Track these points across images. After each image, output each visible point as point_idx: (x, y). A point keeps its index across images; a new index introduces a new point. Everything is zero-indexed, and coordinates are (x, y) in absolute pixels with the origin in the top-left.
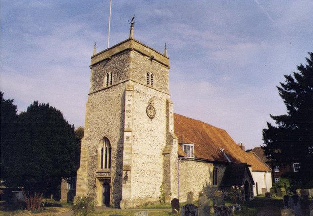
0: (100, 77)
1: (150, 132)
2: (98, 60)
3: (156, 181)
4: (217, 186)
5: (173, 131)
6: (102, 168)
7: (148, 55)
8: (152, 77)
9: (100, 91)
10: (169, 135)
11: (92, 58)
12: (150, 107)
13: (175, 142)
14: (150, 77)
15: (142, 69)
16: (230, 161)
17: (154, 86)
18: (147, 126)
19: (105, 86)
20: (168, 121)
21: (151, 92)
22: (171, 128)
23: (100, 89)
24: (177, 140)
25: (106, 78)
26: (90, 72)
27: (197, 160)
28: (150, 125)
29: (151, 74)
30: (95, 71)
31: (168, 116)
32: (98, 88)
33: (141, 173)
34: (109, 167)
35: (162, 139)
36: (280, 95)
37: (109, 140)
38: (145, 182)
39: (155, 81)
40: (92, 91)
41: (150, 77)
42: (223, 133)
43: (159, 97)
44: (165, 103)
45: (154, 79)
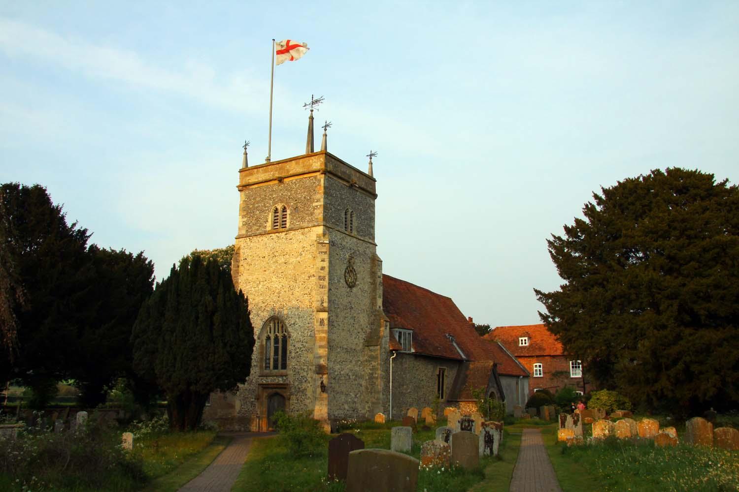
0: (262, 211)
1: (349, 310)
2: (253, 179)
3: (357, 391)
4: (442, 400)
5: (382, 308)
6: (267, 367)
7: (346, 178)
8: (351, 217)
9: (261, 234)
10: (373, 312)
11: (241, 171)
12: (350, 270)
13: (386, 326)
14: (349, 216)
15: (339, 205)
16: (464, 357)
17: (354, 233)
18: (345, 301)
19: (269, 226)
20: (374, 290)
21: (349, 242)
22: (380, 302)
23: (258, 232)
24: (388, 324)
25: (270, 218)
26: (236, 199)
27: (416, 356)
28: (350, 299)
29: (350, 211)
30: (248, 197)
31: (373, 283)
32: (258, 230)
33: (337, 378)
34: (284, 366)
35: (364, 319)
36: (553, 257)
37: (283, 322)
38: (342, 392)
39: (355, 224)
40: (244, 232)
41: (349, 216)
42: (446, 304)
43: (361, 250)
44: (369, 261)
45: (354, 219)
